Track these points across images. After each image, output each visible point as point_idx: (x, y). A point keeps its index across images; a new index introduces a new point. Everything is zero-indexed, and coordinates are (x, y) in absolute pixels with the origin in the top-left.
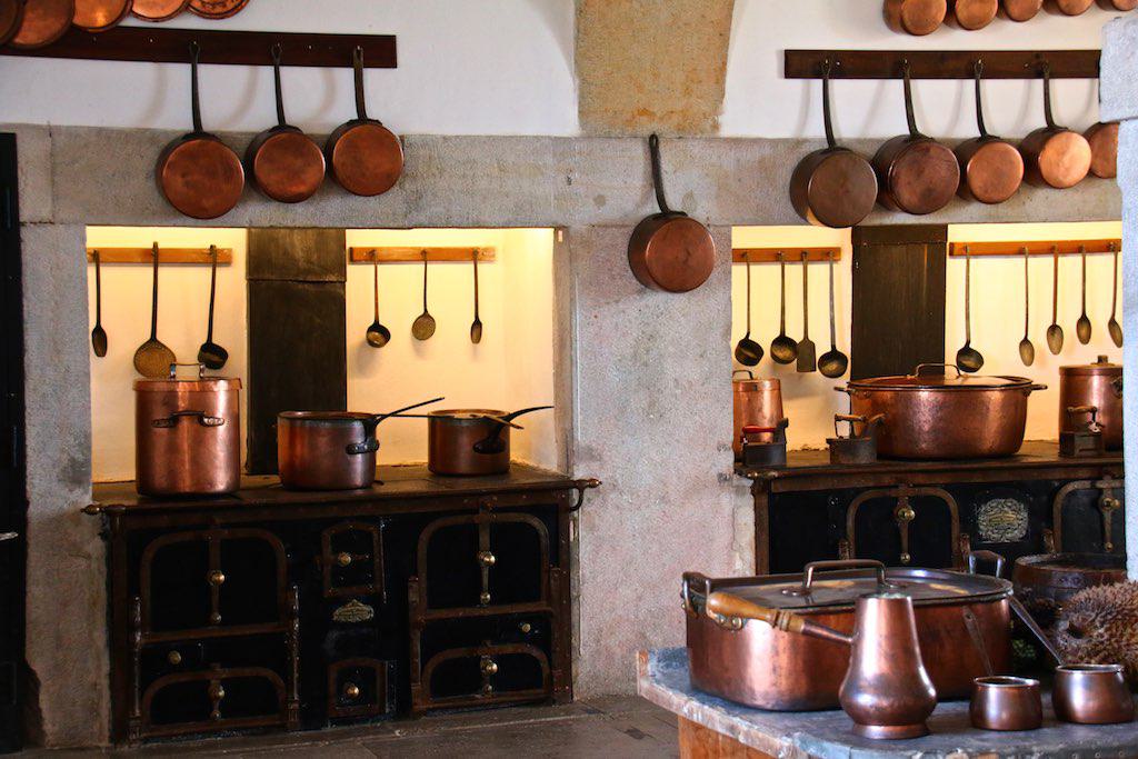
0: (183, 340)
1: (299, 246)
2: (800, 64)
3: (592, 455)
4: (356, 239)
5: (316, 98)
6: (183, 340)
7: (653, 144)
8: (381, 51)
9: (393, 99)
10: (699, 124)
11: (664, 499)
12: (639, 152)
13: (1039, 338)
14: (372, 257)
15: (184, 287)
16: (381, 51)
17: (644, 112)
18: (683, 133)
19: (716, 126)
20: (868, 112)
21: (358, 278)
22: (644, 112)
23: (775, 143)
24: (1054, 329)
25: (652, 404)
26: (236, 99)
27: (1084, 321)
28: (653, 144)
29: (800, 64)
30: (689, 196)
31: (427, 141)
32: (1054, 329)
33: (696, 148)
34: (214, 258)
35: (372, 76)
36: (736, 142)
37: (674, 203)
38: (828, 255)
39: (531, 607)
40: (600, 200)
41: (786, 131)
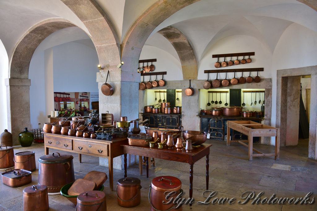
0: (162, 99)
1: (171, 91)
2: (206, 72)
3: (183, 112)
4: (177, 90)
5: (160, 77)
6: (162, 99)
7: (190, 80)
8: (165, 73)
9: (166, 77)
10: (195, 78)
11: (191, 117)
12: (189, 82)
13: (253, 102)
14: (178, 92)
15: (162, 94)
16: (165, 73)
17: (190, 77)
18: (194, 79)
19: (197, 79)
20: (213, 77)
21: (177, 93)
22: (190, 77)
23: (203, 80)
24: (256, 102)
25: (190, 107)
26: (153, 78)
27: (260, 101)
28: (190, 80)
29: (206, 72)
30: (194, 86)
31: (169, 81)
32: (256, 102)
33: (194, 81)
34: (164, 92)
35: (165, 75)
36: (199, 80)
37: (192, 86)
38: (227, 92)
39: (175, 126)
40: (185, 86)
41: (205, 79)
